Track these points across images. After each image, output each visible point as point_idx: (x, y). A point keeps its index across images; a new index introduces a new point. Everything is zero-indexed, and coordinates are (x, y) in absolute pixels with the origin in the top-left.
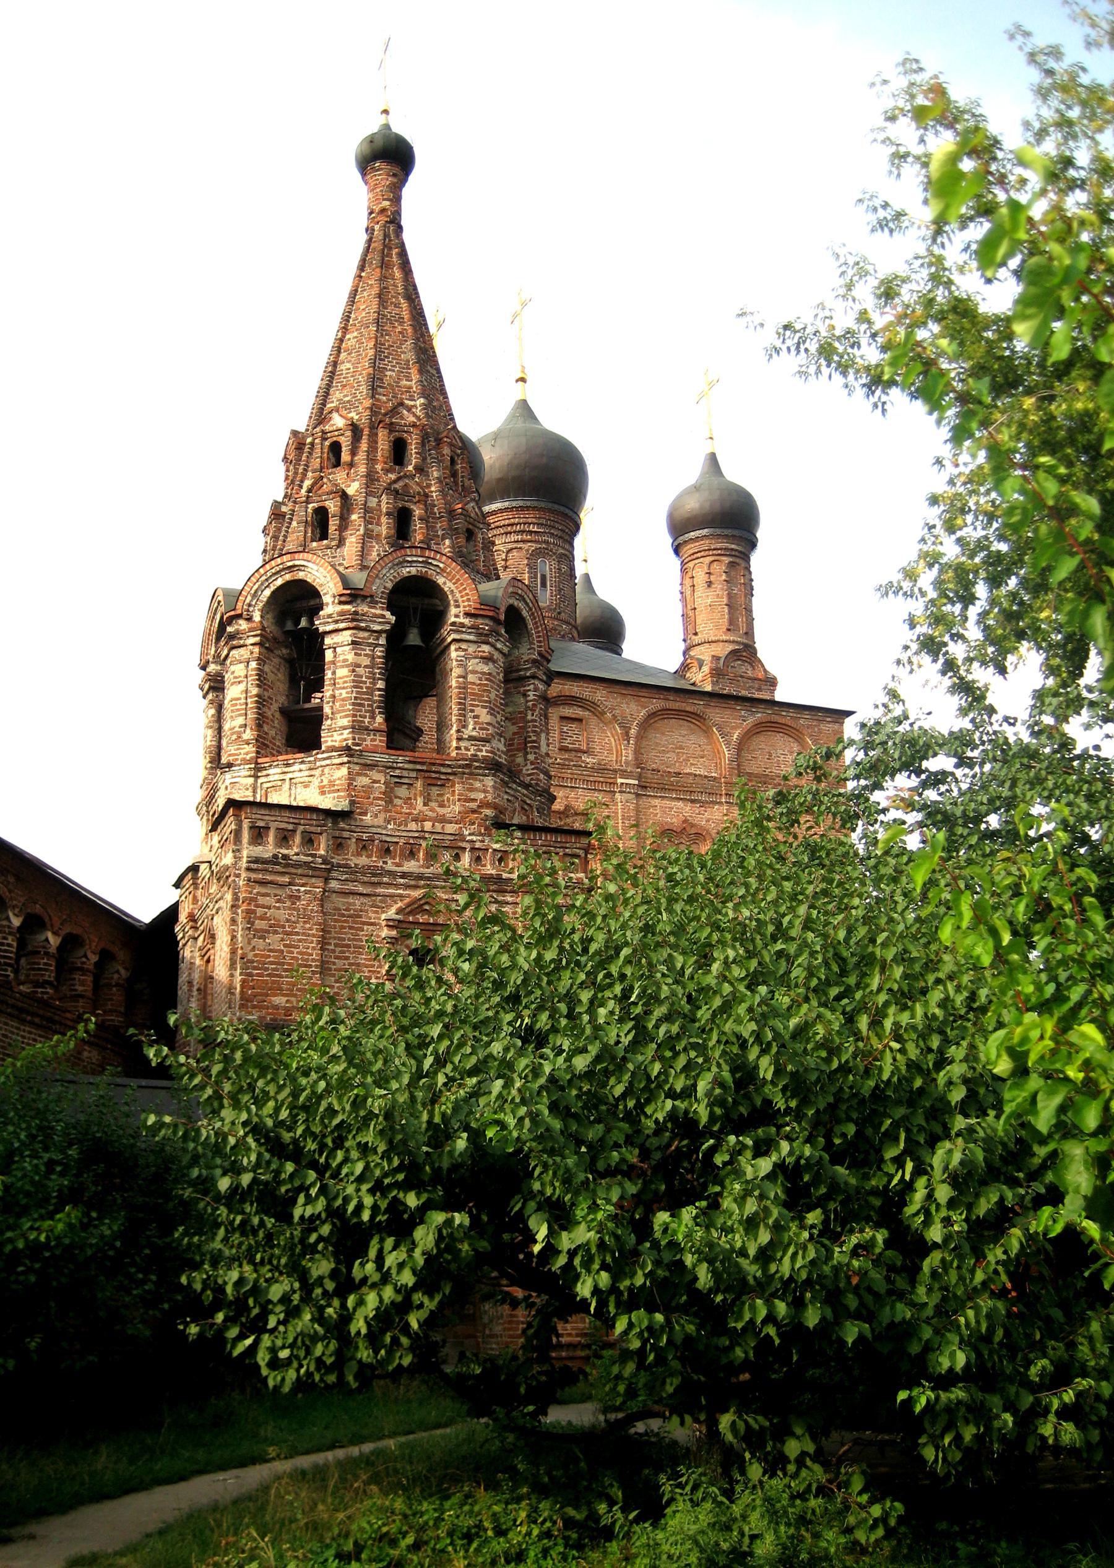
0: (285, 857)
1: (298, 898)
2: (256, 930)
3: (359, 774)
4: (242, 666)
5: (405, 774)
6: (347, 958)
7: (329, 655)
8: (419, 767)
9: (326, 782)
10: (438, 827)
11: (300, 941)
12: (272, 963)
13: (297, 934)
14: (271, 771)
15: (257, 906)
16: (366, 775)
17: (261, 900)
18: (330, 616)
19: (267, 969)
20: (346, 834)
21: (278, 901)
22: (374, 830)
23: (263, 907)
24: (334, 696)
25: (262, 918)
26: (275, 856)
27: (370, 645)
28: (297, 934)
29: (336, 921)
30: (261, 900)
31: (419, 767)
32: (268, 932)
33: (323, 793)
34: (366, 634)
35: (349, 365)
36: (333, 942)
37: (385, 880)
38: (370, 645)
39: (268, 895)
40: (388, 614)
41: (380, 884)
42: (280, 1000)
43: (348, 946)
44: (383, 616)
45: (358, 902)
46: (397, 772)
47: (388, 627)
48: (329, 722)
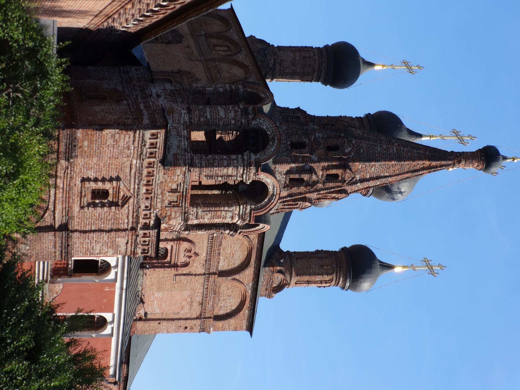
0: (145, 145)
1: (128, 149)
2: (115, 134)
3: (181, 171)
4: (233, 116)
5: (182, 188)
6: (104, 167)
7: (234, 157)
8: (184, 193)
9: (178, 157)
10: (159, 200)
11: (111, 150)
12: (101, 141)
13: (113, 149)
14: (185, 131)
15: (125, 135)
16: (181, 173)
17: (127, 137)
18: (250, 158)
19: (99, 139)
20: (155, 166)
21: (127, 143)
22: (158, 176)
23: (124, 137)
24: (215, 159)
25: (120, 136)
26: (145, 142)
27: (237, 174)
28: (113, 149)
29: (119, 162)
30: (127, 137)
31: (184, 193)
32: (114, 139)
33: (174, 155)
34: (241, 172)
35: (379, 150)
36: (111, 162)
37: (137, 181)
38: (237, 174)
39: (129, 138)
40: (251, 181)
41: (135, 178)
42: (86, 143)
43: (109, 167)
44: (249, 179)
45: (128, 170)
46: (182, 185)
47: (244, 181)
48: (204, 157)
